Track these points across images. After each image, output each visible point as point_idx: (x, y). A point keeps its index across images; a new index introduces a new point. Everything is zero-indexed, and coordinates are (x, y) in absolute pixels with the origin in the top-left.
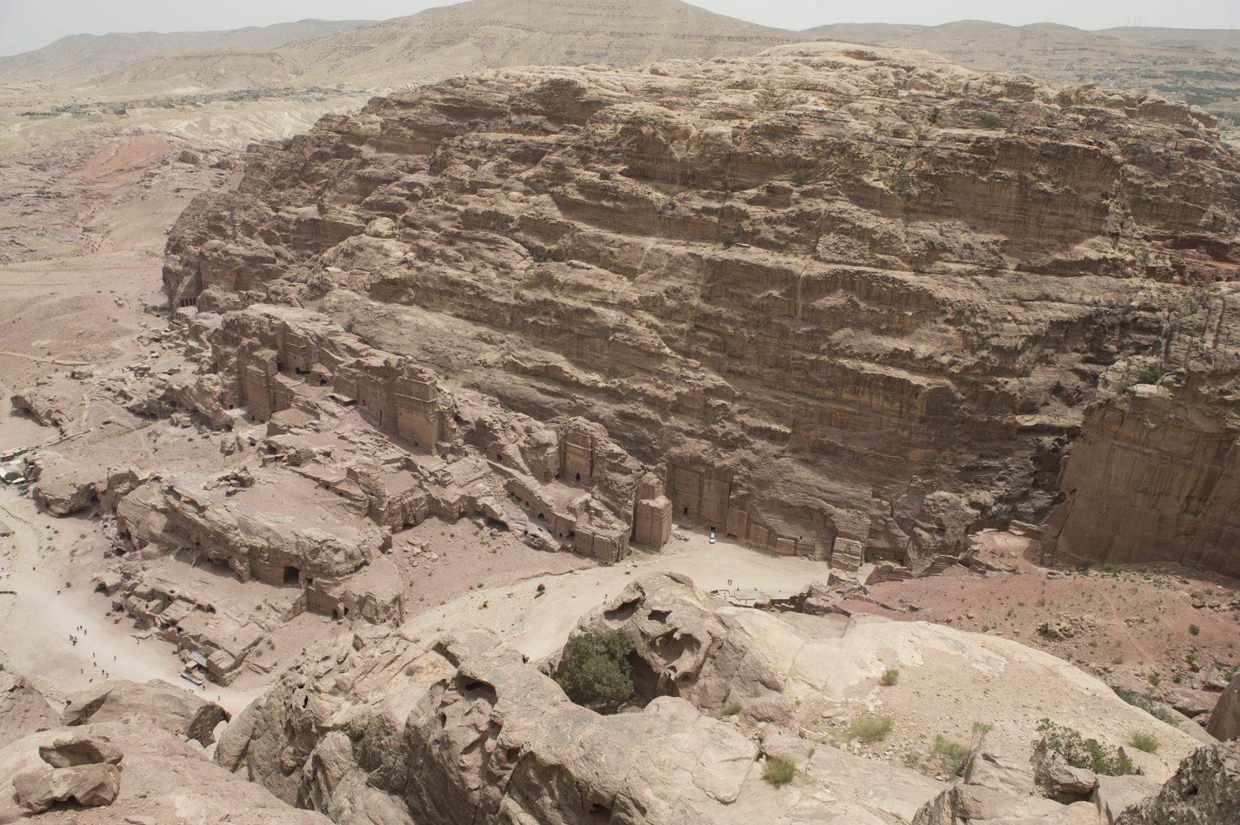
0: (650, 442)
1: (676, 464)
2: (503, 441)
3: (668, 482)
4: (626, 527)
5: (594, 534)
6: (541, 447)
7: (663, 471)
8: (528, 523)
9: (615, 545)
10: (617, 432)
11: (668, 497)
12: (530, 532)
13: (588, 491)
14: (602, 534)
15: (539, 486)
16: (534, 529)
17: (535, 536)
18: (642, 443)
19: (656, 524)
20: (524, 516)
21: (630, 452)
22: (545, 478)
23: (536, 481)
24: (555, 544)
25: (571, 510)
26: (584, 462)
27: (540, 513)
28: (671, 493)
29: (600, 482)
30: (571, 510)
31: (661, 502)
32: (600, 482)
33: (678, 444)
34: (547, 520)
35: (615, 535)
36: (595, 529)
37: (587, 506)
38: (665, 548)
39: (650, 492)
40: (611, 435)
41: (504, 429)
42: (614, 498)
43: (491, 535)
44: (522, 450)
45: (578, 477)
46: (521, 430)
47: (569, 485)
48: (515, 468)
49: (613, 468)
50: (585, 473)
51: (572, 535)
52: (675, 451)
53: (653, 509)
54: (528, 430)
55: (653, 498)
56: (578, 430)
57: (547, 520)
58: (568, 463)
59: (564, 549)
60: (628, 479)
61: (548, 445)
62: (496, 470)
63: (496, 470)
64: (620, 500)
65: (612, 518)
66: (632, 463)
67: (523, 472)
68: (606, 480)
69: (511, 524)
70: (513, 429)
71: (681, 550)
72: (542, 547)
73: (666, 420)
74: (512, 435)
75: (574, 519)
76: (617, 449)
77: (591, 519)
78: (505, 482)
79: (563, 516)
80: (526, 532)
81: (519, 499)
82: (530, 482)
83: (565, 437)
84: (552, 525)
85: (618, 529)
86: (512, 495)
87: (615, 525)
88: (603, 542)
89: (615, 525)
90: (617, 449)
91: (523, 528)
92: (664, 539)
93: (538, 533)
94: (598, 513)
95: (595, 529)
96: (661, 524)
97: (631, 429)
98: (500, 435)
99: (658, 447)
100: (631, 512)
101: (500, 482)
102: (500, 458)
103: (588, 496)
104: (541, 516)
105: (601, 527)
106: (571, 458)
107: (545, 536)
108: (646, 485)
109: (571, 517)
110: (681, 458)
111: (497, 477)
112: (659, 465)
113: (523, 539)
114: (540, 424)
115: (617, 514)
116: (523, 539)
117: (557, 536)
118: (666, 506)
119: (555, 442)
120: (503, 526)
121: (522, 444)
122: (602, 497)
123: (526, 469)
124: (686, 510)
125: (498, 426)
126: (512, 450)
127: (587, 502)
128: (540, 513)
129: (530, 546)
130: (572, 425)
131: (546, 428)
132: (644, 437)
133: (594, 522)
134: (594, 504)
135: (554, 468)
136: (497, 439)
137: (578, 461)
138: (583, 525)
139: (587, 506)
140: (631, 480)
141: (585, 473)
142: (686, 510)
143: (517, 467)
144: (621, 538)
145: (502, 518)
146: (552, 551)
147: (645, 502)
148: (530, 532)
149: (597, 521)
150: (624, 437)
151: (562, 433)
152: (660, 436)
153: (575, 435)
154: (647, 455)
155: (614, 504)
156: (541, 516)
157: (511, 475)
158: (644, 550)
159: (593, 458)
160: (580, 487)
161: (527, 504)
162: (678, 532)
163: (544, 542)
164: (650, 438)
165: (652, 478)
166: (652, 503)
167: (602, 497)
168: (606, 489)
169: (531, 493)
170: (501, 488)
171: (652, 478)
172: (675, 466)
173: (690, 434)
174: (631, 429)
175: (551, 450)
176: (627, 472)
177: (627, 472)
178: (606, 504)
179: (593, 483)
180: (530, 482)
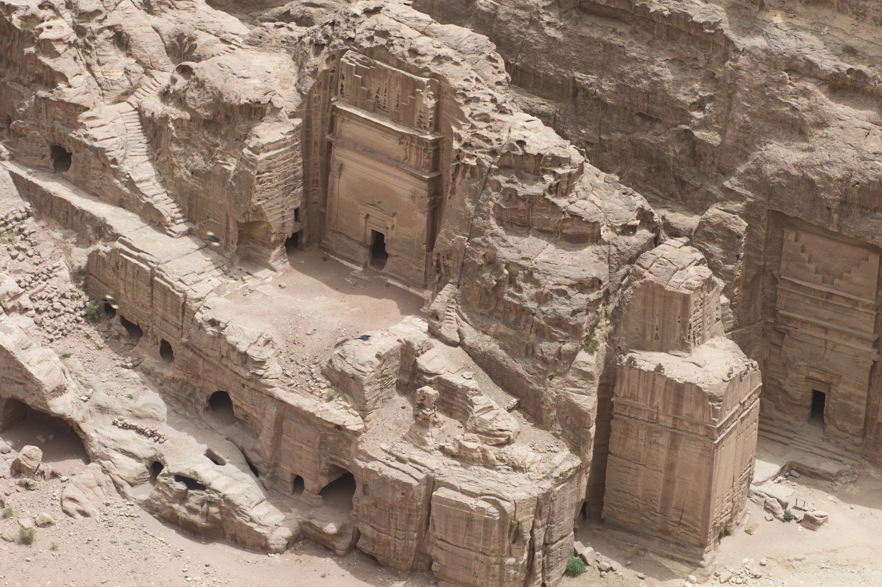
0: (682, 113)
1: (786, 211)
2: (76, 88)
3: (749, 284)
4: (565, 460)
5: (432, 483)
6: (229, 119)
7: (729, 238)
8: (164, 429)
9: (517, 534)
10: (548, 67)
11: (745, 346)
12: (173, 465)
13: (413, 305)
14: (464, 486)
15: (214, 279)
16: (187, 452)
17: (192, 483)
18: (649, 118)
19: (689, 452)
20: (152, 400)
21: (598, 154)
22: (241, 245)
23: (202, 261)
24: (270, 518)
25: (343, 383)
26: (406, 187)
27: (214, 390)
28: (760, 325)
29: (467, 271)
30: (343, 383)
31: (714, 362)
32: (467, 271)
33: (796, 129)
34: (246, 423)
35: (518, 490)
36: (435, 462)
37: (407, 372)
38: (722, 555)
39: (668, 321)
40: (522, 78)
41: (84, 40)
42: (523, 341)
43: (18, 469)
44: (153, 129)
45: (378, 248)
46: (152, 46)
47: (342, 282)
48: (121, 203)
49: (522, 217)
50: (407, 228)
51: (342, 483)
52: (782, 154)
53: (679, 391)
54: (181, 49)
55: (684, 346)
56: (383, 53)
57: (246, 423)
58: (341, 186)
59: (307, 540)
60: (584, 262)
61: (256, 111)
62: (46, 207)
63: (46, 207)
64: (548, 348)
65: (511, 422)
66: (601, 197)
67: (154, 219)
68: (492, 263)
69: (98, 431)
70: (121, 40)
71: (791, 564)
72: (219, 526)
73: (752, 28)
74: (116, 65)
75: (352, 422)
76: (541, 139)
77: (423, 422)
78: (80, 256)
79: (308, 404)
80: (156, 466)
81: (134, 330)
82: (179, 259)
83: (329, 82)
84: (265, 441)
85: (535, 467)
86: (101, 313)
87: (518, 451)
88: (468, 519)
89: (518, 451)
90: (541, 139)
91: (144, 447)
92: (718, 512)
93: (206, 471)
94: (453, 400)
95: (435, 462)
96: (709, 454)
97: (607, 58)
98: (65, 63)
99: (712, 137)
100: (588, 402)
101: (60, 259)
102: (60, 158)
103: (414, 328)
104: (220, 402)
105: (462, 456)
106: (354, 170)
107: (233, 483)
108: (653, 290)
109: (338, 412)
110: (804, 185)
111: (48, 239)
112: (714, 211)
113: (145, 492)
114: (231, 24)
115: (530, 407)
116: (145, 492)
117: (281, 484)
118: (735, 380)
119: (287, 98)
120: (65, 438)
121: (155, 106)
122: (472, 336)
123: (167, 207)
124: (818, 400)
125: (59, 28)
126: (111, 127)
127: (407, 353)
128: (214, 390)
129: (171, 520)
130: (360, 33)
131: (255, 42)
132: (655, 91)
133: (433, 437)
134: (438, 360)
135: (277, 210)
136: (52, 79)
137: (377, 178)
138: (388, 444)
139: (407, 372)
140: (599, 271)
141: (407, 228)
142: (818, 400)
143: (130, 199)
144: (542, 505)
145: (59, 406)
146: (259, 545)
147: (647, 360)
148: (173, 465)
149: (448, 430)
150: (577, 89)
151: (319, 62)
152: (725, 88)
153: (367, 72)
154: (668, 171)
155: (519, 367)
156: (220, 402)
157: (102, 230)
158: (631, 559)
159: (440, 171)
160: (381, 290)
161: (166, 350)
162: (784, 491)
163: (229, 506)
164: (683, 97)
165: (679, 265)
166: (677, 367)
167: (472, 336)
168: (492, 297)
169: (183, 308)
170: (63, 281)
171: (679, 265)
172: (780, 220)
173: (844, 87)
174: (607, 58)
175: (268, 133)
176: (578, 233)
177: (578, 233)
178: (484, 362)
179: (436, 275)
180: (179, 259)
